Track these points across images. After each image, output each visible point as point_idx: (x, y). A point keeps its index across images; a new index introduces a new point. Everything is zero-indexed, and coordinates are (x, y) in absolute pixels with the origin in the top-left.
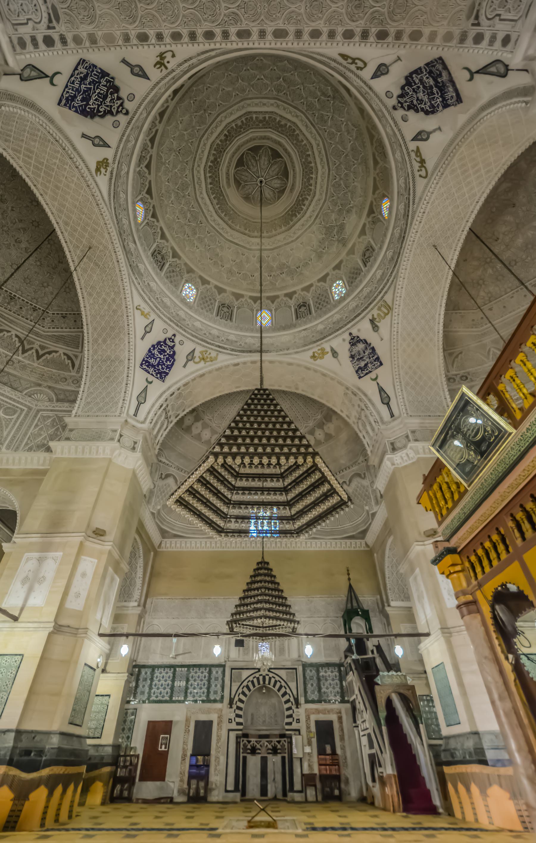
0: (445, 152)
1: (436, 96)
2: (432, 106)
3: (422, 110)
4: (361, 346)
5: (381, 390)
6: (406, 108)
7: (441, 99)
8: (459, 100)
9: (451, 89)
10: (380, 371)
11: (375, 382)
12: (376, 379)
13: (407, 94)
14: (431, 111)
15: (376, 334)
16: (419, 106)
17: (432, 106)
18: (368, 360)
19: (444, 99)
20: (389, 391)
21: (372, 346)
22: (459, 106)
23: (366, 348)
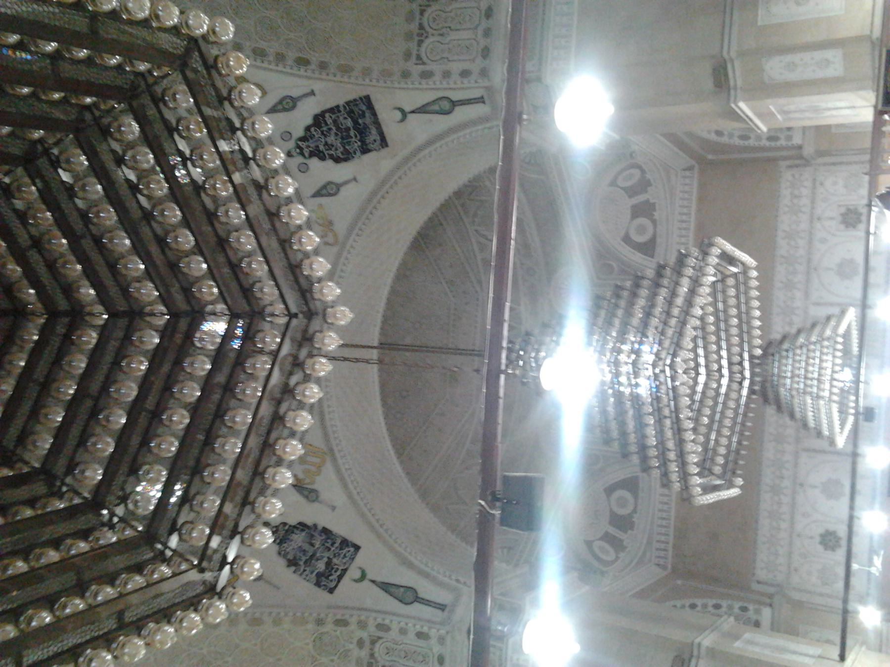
0: (362, 210)
1: (354, 139)
2: (346, 152)
3: (332, 157)
4: (298, 539)
5: (386, 587)
6: (307, 155)
7: (359, 143)
8: (384, 143)
9: (374, 131)
10: (361, 559)
11: (366, 583)
12: (363, 577)
13: (312, 137)
14: (345, 157)
15: (316, 505)
16: (326, 153)
17: (346, 152)
18: (326, 554)
19: (363, 142)
20: (405, 578)
21: (320, 528)
22: (384, 152)
23: (312, 536)
